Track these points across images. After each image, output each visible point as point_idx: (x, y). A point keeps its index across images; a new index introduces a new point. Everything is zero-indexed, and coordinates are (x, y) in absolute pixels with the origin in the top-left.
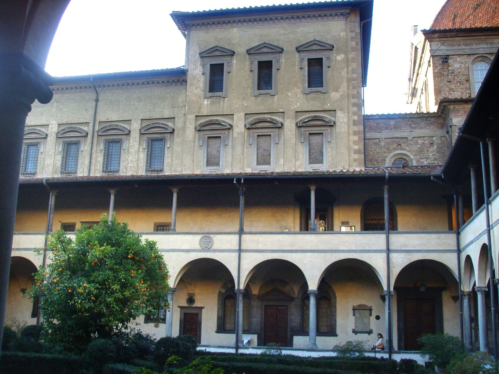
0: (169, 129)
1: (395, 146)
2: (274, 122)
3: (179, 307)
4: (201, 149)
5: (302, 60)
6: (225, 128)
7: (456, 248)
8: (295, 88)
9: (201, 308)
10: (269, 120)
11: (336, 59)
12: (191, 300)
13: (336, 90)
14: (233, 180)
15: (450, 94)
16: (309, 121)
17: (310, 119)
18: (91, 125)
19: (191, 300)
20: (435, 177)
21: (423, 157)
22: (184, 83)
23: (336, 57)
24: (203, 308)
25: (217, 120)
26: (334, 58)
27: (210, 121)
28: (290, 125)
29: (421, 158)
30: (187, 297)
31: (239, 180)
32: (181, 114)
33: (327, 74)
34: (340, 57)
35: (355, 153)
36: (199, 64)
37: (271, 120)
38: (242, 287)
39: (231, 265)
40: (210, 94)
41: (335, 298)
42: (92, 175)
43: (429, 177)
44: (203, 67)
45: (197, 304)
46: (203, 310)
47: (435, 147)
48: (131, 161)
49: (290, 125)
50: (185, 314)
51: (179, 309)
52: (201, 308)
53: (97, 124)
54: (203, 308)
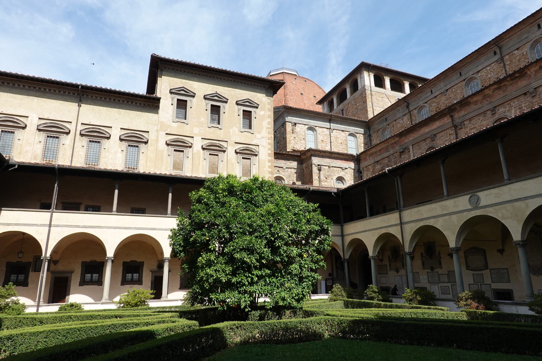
0: (145, 139)
1: (276, 171)
2: (222, 147)
3: (151, 271)
4: (169, 157)
5: (239, 110)
6: (188, 145)
7: (341, 234)
8: (235, 127)
10: (218, 145)
11: (259, 113)
13: (259, 133)
15: (295, 145)
17: (244, 148)
18: (74, 124)
20: (334, 193)
21: (291, 180)
22: (156, 108)
23: (259, 112)
26: (258, 113)
28: (231, 150)
29: (289, 180)
32: (154, 130)
33: (254, 122)
34: (262, 113)
35: (269, 173)
36: (169, 96)
37: (219, 145)
38: (48, 255)
39: (42, 240)
40: (177, 120)
42: (73, 165)
43: (331, 193)
44: (172, 99)
48: (111, 158)
49: (231, 150)
50: (155, 277)
51: (51, 273)
53: (79, 124)
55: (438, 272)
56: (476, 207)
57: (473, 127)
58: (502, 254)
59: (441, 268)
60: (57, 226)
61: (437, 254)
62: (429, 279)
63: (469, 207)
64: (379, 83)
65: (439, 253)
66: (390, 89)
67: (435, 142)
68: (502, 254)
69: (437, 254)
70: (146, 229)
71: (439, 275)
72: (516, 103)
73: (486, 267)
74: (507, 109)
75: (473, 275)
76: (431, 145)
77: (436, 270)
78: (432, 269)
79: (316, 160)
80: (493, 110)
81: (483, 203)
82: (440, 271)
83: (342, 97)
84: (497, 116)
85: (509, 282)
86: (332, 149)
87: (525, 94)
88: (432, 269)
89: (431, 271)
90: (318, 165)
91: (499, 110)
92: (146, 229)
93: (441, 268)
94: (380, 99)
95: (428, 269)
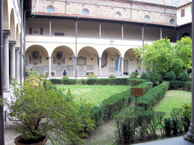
55: (62, 66)
56: (111, 45)
57: (74, 6)
59: (64, 64)
61: (63, 57)
62: (57, 69)
63: (110, 44)
65: (64, 58)
67: (53, 4)
69: (63, 57)
71: (62, 67)
72: (92, 6)
73: (85, 64)
74: (89, 7)
75: (79, 67)
76: (51, 4)
77: (61, 65)
78: (59, 64)
80: (83, 5)
81: (114, 43)
82: (63, 65)
84: (84, 8)
85: (93, 70)
87: (96, 5)
88: (59, 64)
89: (58, 65)
91: (85, 5)
93: (64, 64)
95: (56, 64)
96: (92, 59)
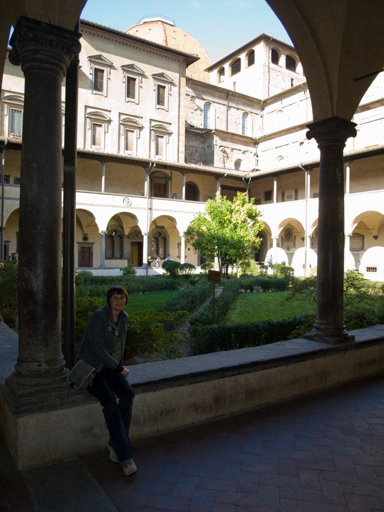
6: (106, 119)
9: (92, 244)
12: (85, 238)
14: (149, 163)
16: (158, 127)
19: (85, 238)
24: (94, 243)
25: (101, 113)
27: (97, 112)
30: (82, 236)
31: (153, 164)
41: (169, 238)
45: (90, 241)
46: (94, 245)
47: (198, 153)
50: (81, 247)
52: (92, 244)
54: (94, 243)
58: (376, 239)
60: (9, 198)
64: (275, 60)
66: (285, 67)
68: (376, 239)
70: (85, 204)
79: (217, 141)
83: (236, 68)
86: (229, 128)
90: (221, 146)
92: (85, 204)
94: (275, 77)
96: (376, 237)
